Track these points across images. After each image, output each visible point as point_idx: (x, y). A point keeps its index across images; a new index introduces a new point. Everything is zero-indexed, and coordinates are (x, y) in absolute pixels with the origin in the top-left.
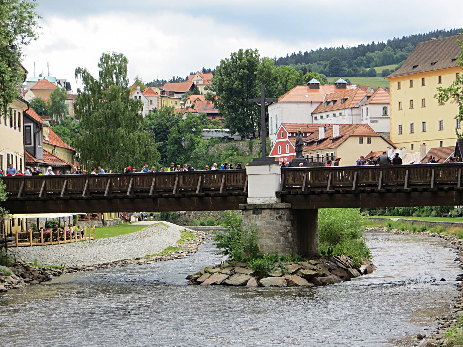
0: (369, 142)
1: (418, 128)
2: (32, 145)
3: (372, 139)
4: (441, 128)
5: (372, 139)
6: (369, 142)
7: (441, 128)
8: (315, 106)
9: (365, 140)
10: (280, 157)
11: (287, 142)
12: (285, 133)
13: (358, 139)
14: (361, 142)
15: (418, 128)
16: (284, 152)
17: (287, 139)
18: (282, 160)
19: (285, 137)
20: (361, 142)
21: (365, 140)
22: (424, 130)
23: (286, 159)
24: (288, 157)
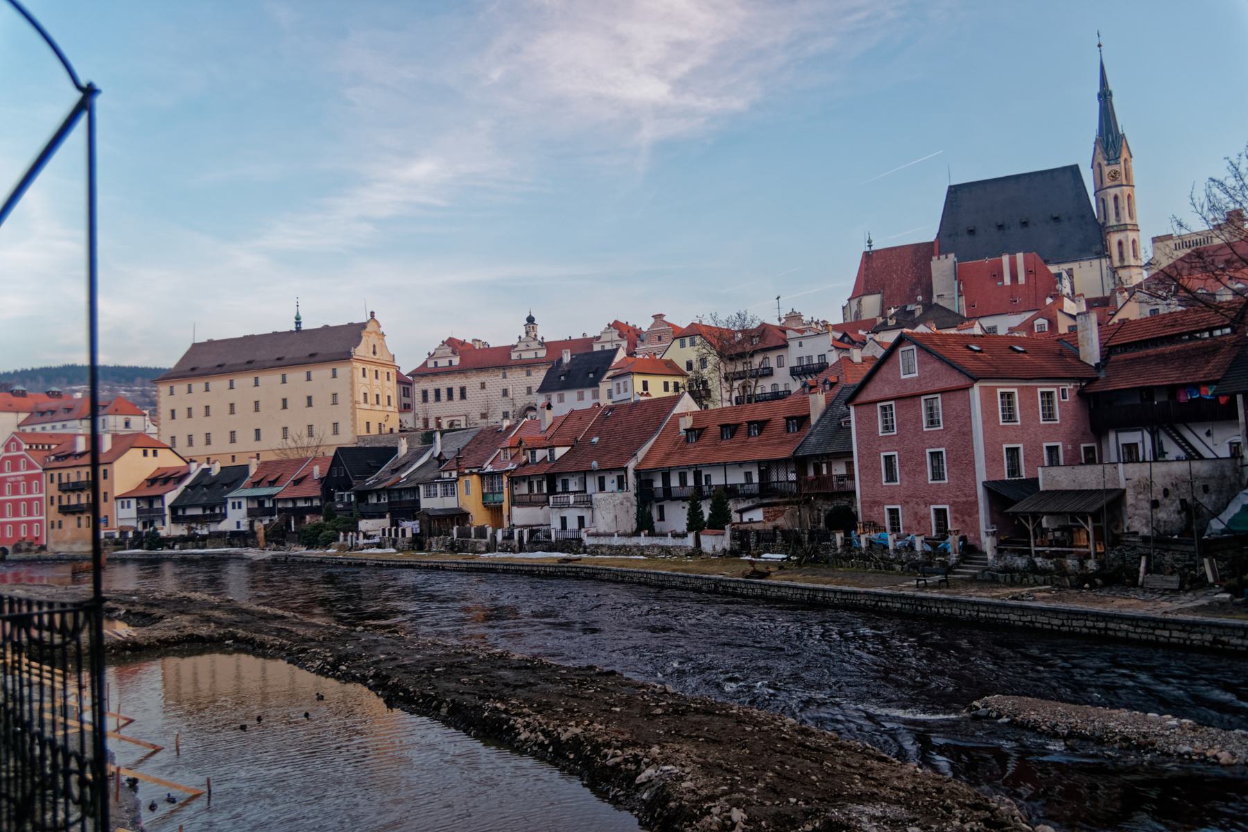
0: (155, 454)
1: (199, 440)
3: (159, 451)
4: (233, 440)
5: (159, 451)
6: (155, 454)
7: (233, 440)
8: (23, 416)
9: (150, 451)
11: (22, 456)
13: (141, 451)
14: (145, 454)
15: (199, 440)
18: (13, 479)
20: (145, 454)
21: (150, 451)
22: (208, 442)
23: (20, 479)
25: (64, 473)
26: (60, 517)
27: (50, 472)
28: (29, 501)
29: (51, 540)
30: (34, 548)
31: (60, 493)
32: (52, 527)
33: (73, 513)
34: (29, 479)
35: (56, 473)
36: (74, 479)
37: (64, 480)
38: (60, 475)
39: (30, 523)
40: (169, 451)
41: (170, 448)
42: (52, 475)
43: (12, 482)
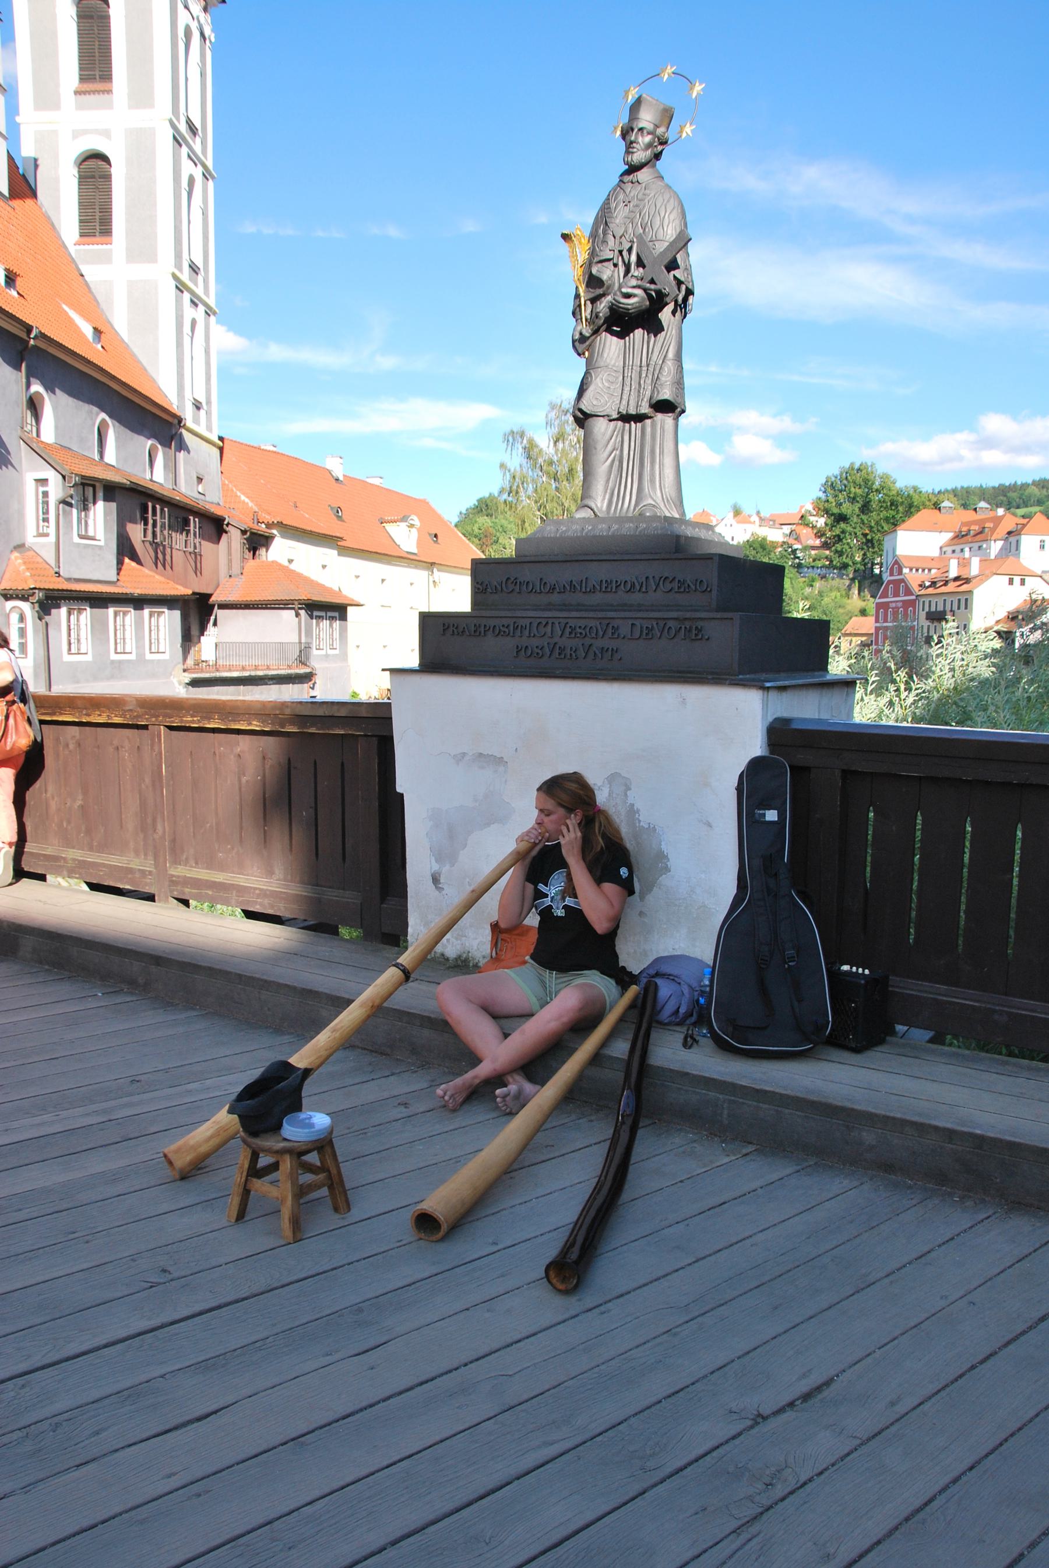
0: (1023, 583)
6: (1023, 583)
9: (1017, 580)
10: (891, 602)
14: (1011, 582)
16: (896, 594)
18: (894, 605)
20: (1011, 582)
21: (1017, 580)
23: (900, 604)
25: (934, 600)
31: (928, 623)
37: (933, 609)
38: (930, 602)
40: (1039, 579)
41: (1041, 577)
42: (924, 602)
43: (893, 608)
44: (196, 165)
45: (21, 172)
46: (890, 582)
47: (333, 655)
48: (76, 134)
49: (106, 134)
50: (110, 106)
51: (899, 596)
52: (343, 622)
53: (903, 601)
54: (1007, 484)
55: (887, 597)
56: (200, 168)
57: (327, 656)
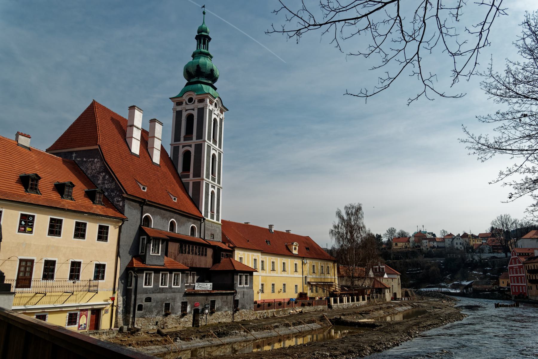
2: (144, 254)
11: (517, 258)
12: (515, 253)
16: (516, 263)
17: (516, 257)
18: (515, 267)
19: (516, 255)
23: (517, 267)
24: (518, 266)
25: (530, 265)
26: (529, 285)
27: (525, 265)
28: (517, 277)
29: (529, 294)
30: (525, 297)
31: (528, 274)
32: (529, 289)
33: (535, 283)
34: (520, 267)
35: (527, 265)
36: (533, 268)
38: (528, 266)
39: (519, 286)
42: (526, 266)
44: (216, 151)
45: (169, 156)
46: (513, 259)
47: (246, 287)
48: (183, 147)
49: (190, 146)
50: (192, 140)
51: (516, 264)
52: (251, 277)
53: (518, 266)
54: (411, 232)
55: (512, 264)
56: (218, 151)
57: (244, 287)
